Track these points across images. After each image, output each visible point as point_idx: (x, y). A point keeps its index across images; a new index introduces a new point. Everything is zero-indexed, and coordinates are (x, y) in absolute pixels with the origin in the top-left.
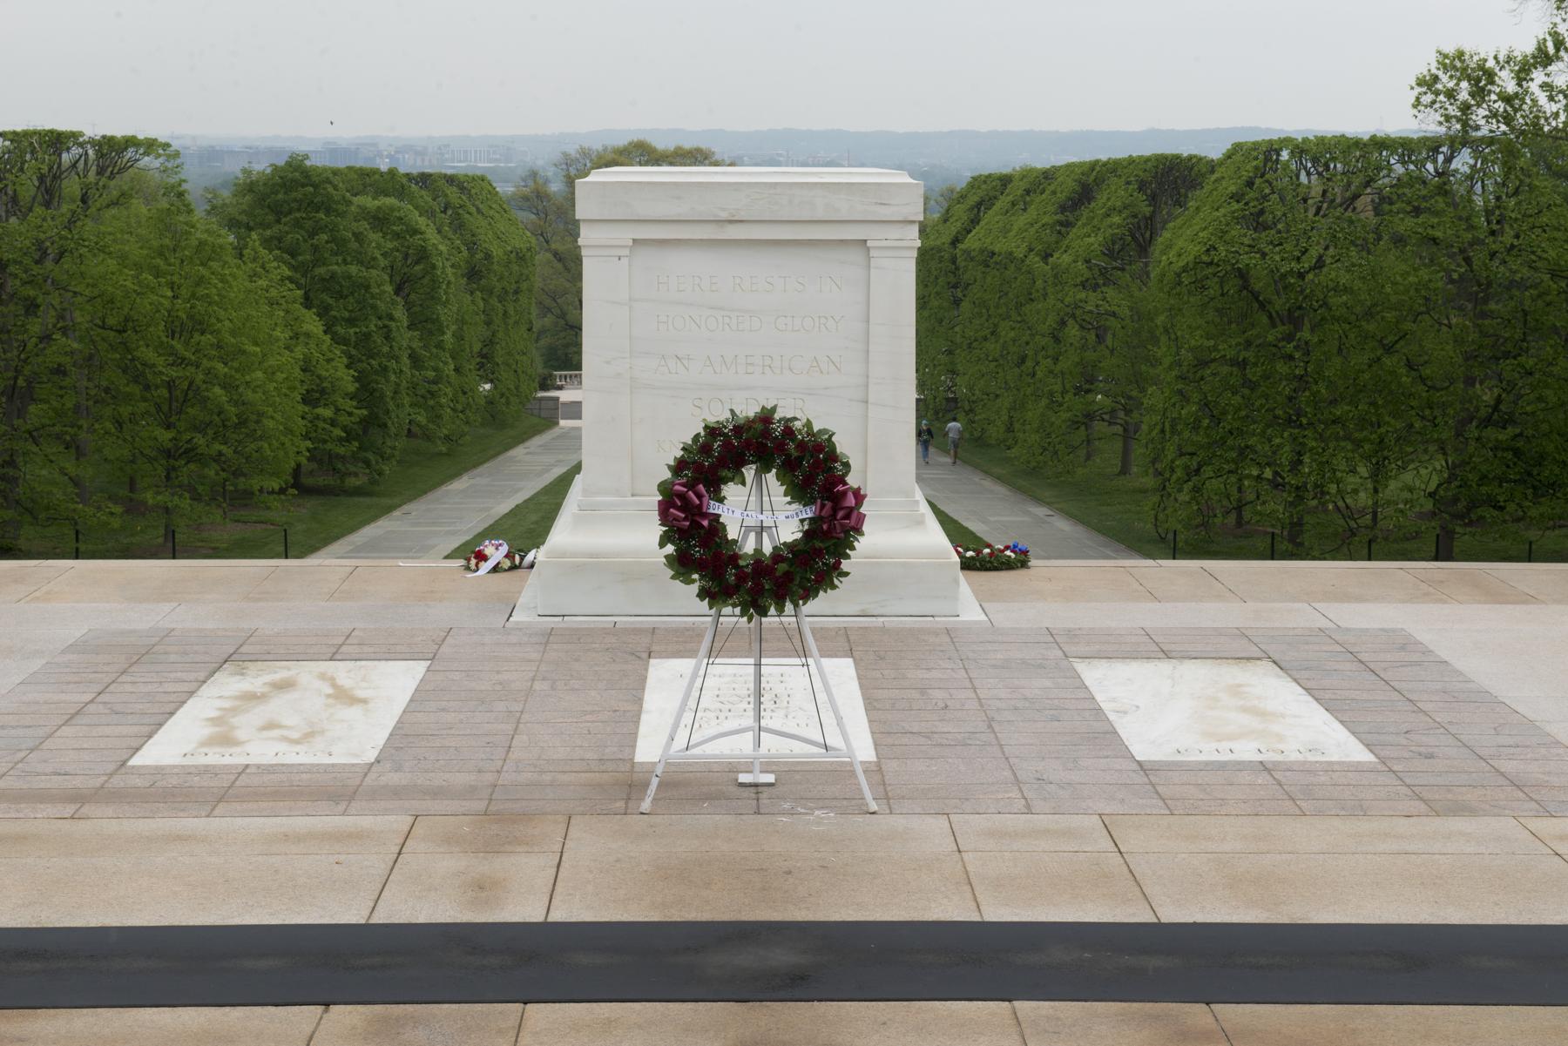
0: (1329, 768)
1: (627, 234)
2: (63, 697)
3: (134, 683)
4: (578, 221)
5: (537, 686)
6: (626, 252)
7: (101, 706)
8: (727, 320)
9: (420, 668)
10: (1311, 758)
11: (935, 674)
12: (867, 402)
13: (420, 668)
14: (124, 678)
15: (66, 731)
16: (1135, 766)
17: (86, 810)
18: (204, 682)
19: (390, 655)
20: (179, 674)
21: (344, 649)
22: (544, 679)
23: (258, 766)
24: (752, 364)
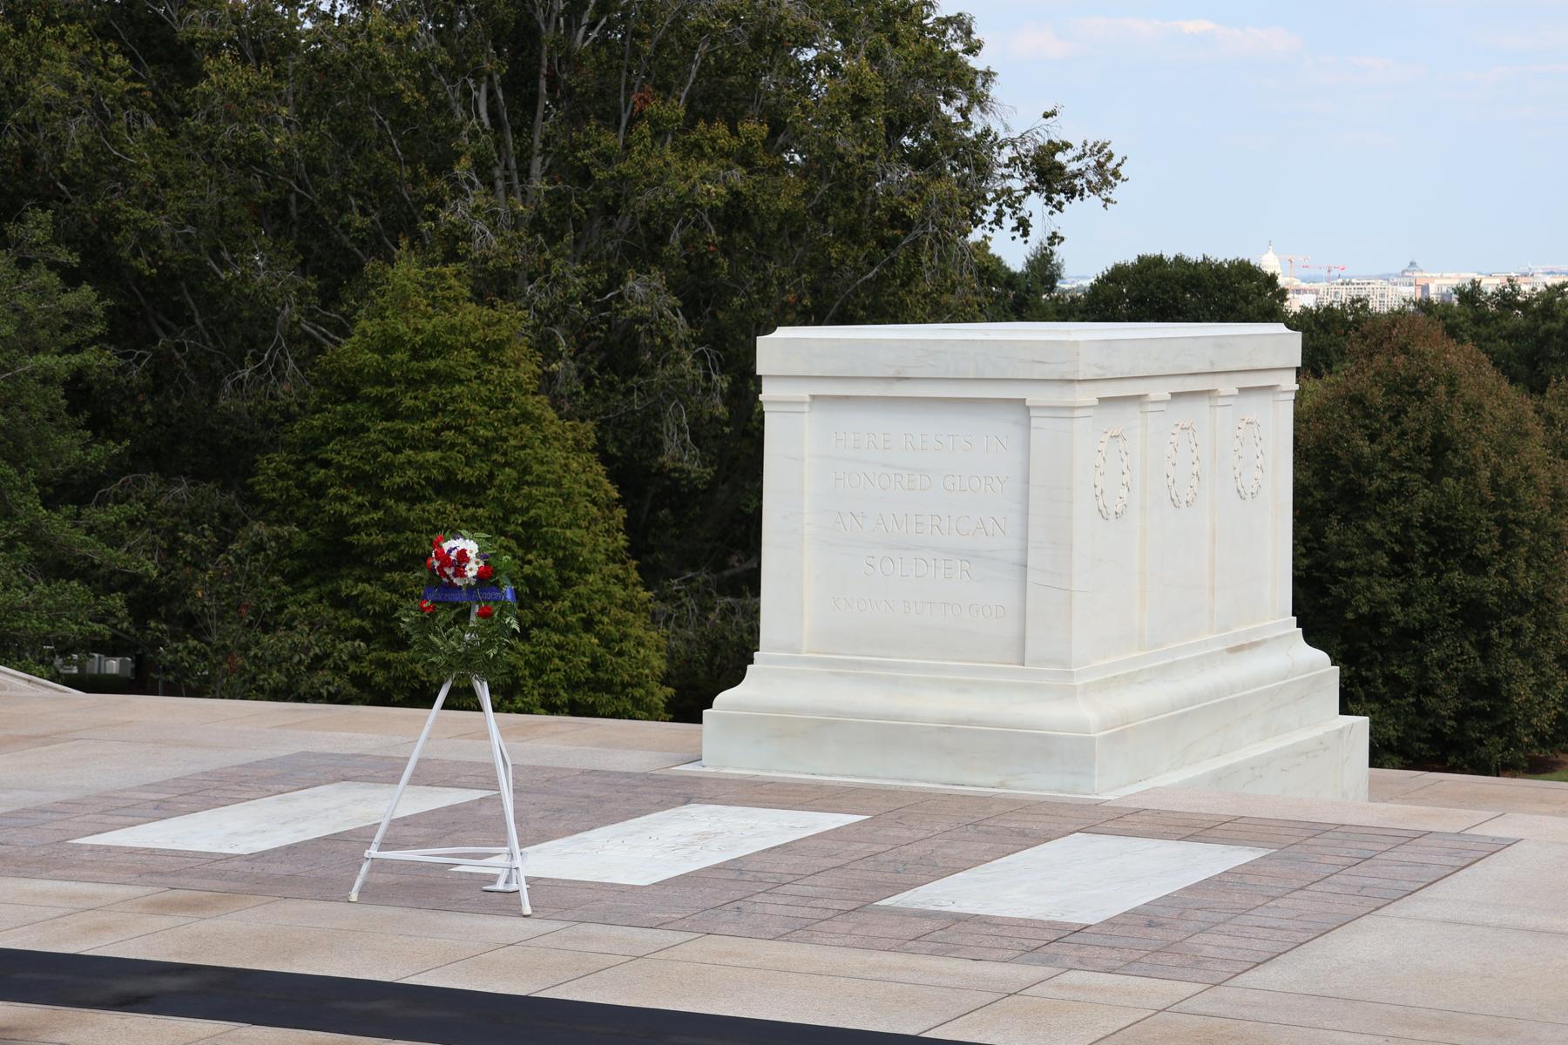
4: (760, 376)
6: (806, 408)
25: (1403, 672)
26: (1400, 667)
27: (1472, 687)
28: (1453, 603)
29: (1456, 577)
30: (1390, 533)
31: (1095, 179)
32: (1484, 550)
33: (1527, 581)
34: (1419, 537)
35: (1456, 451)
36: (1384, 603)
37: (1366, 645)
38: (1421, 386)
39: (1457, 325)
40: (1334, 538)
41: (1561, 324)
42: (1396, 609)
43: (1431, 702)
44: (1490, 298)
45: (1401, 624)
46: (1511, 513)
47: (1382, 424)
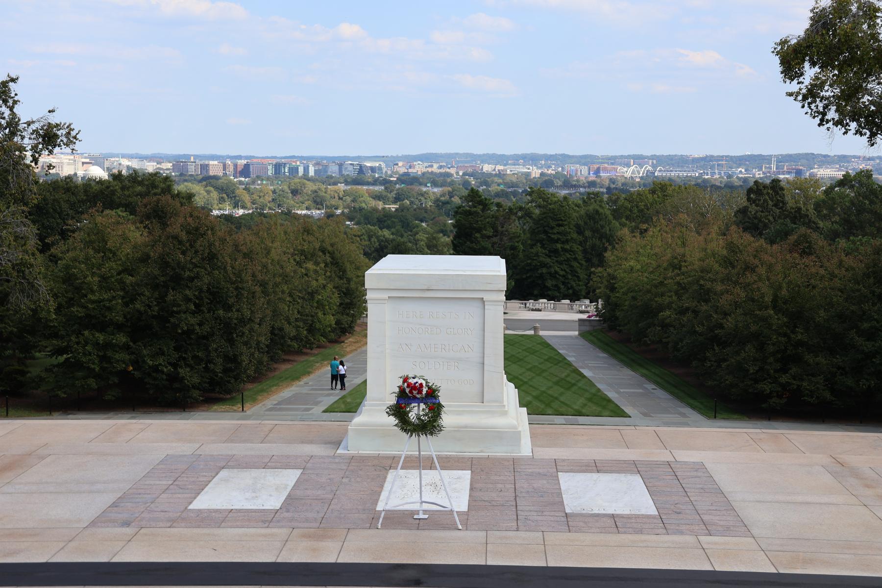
0: (637, 517)
1: (385, 295)
2: (161, 482)
3: (187, 477)
5: (344, 480)
7: (176, 487)
8: (427, 329)
9: (298, 473)
10: (633, 513)
11: (502, 478)
12: (484, 364)
13: (298, 473)
14: (183, 475)
15: (163, 496)
16: (564, 515)
17: (174, 525)
18: (214, 477)
19: (287, 467)
20: (204, 474)
21: (269, 464)
22: (347, 477)
23: (236, 510)
24: (437, 348)
25: (200, 354)
26: (198, 352)
27: (227, 359)
28: (220, 324)
29: (221, 312)
30: (194, 295)
31: (65, 140)
32: (231, 301)
33: (247, 313)
34: (205, 296)
35: (217, 259)
36: (192, 325)
37: (184, 343)
38: (202, 231)
39: (116, 190)
40: (172, 298)
41: (160, 190)
42: (197, 327)
43: (211, 366)
44: (126, 179)
45: (199, 334)
46: (240, 285)
47: (187, 247)
